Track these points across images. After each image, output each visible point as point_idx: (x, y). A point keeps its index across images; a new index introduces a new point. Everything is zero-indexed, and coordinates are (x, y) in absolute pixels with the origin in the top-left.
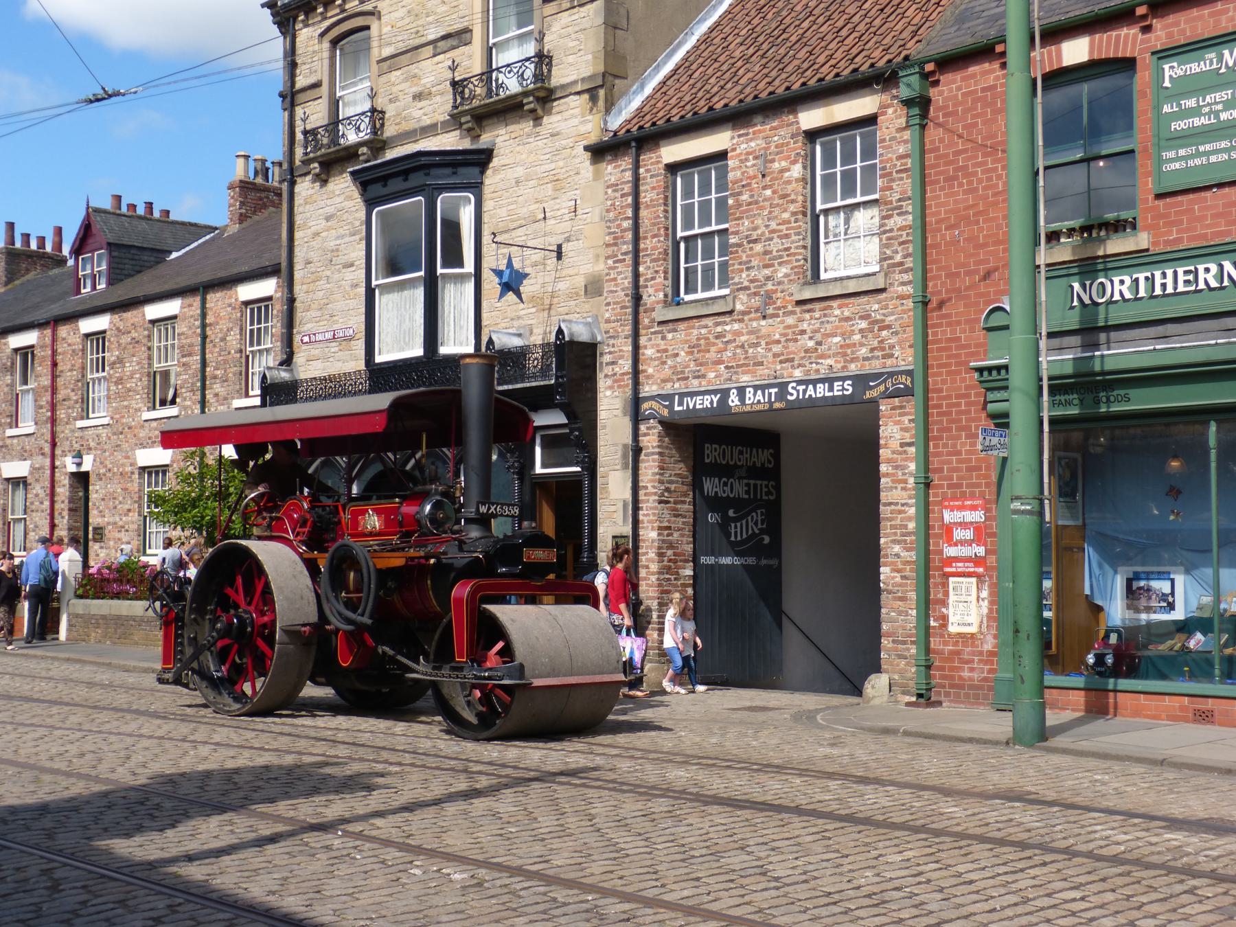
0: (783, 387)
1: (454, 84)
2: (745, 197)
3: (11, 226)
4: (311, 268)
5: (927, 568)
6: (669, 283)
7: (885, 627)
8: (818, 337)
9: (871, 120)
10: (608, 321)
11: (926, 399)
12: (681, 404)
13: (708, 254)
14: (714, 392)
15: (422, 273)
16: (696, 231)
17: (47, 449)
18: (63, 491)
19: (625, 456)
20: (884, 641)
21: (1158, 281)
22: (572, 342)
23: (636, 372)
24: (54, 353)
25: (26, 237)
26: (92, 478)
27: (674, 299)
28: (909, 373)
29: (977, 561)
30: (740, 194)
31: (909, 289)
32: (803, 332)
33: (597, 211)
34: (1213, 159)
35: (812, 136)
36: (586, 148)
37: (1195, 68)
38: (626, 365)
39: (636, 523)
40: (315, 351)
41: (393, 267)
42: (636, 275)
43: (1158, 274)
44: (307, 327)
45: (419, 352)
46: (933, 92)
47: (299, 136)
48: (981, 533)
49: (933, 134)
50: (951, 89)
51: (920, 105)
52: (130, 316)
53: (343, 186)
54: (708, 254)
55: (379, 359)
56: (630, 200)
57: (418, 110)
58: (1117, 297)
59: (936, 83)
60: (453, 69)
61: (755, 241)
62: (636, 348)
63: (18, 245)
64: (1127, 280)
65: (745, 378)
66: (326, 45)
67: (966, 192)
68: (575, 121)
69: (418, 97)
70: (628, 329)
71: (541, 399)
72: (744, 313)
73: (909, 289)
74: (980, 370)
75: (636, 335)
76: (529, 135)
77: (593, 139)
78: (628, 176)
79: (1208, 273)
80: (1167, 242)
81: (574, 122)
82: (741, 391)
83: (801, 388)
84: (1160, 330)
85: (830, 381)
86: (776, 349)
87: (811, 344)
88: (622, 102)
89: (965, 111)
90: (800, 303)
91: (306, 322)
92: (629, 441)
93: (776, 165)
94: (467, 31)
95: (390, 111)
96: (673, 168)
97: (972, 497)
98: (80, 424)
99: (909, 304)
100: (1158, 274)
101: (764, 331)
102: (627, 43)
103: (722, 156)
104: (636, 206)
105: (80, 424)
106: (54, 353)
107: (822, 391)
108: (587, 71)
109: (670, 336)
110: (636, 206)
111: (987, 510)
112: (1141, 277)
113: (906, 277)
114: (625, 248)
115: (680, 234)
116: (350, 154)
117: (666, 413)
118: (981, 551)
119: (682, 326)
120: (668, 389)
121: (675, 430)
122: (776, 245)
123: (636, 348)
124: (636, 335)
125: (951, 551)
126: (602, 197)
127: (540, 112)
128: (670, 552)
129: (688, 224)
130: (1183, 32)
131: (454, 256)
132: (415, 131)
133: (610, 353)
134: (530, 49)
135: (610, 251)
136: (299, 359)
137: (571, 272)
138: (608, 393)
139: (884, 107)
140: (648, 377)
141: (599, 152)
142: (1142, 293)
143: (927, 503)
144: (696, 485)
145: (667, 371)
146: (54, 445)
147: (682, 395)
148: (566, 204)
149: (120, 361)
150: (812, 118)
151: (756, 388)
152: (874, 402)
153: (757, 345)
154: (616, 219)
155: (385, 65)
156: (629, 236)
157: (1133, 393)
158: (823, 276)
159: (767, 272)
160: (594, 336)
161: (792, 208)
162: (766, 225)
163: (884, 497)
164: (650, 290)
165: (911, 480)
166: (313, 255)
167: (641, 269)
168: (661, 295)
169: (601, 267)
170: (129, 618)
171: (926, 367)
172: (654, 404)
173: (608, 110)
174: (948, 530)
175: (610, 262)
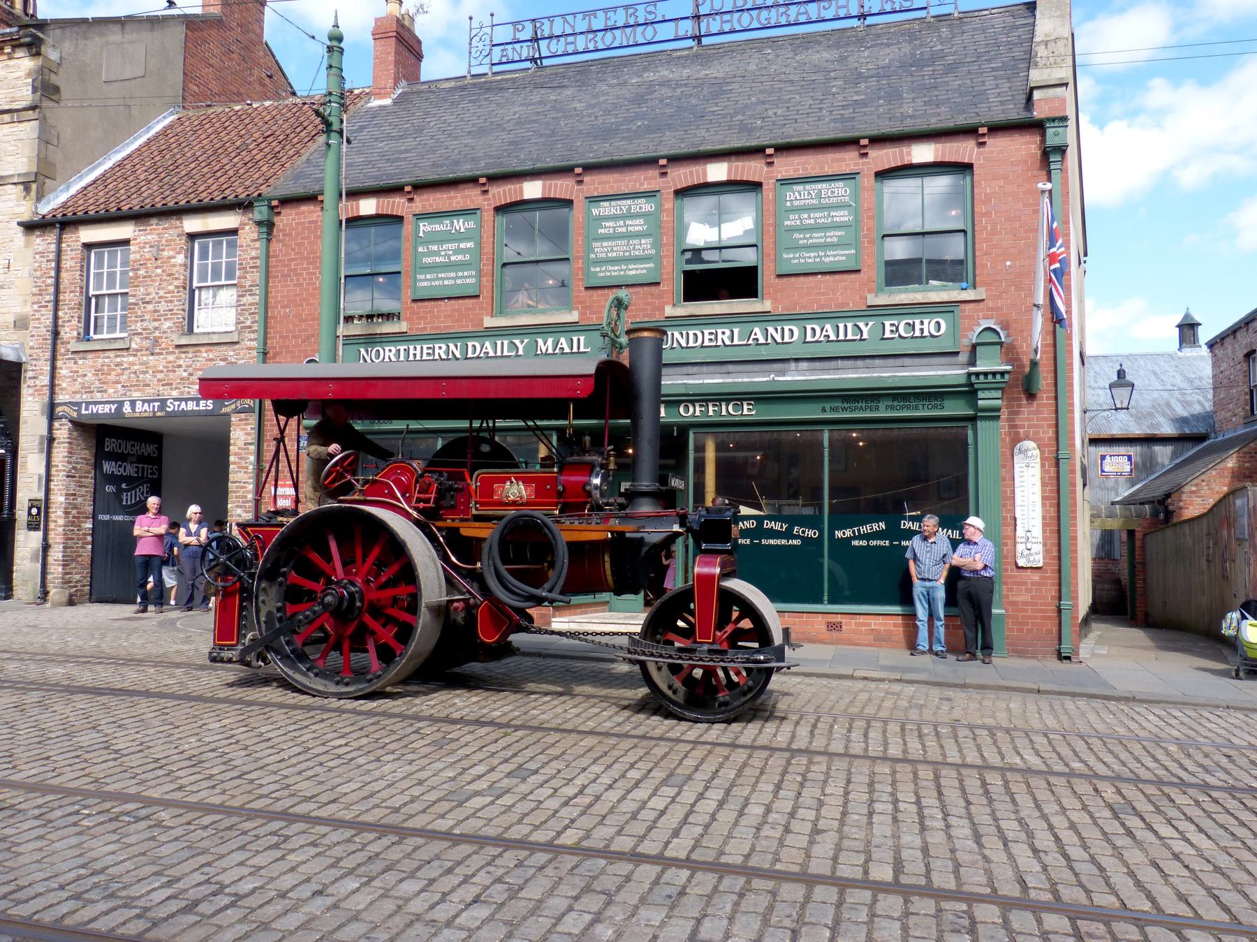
0: (163, 402)
2: (142, 272)
6: (82, 325)
8: (190, 370)
9: (234, 232)
10: (31, 348)
12: (87, 409)
14: (113, 402)
16: (104, 291)
19: (41, 443)
21: (412, 352)
23: (52, 386)
27: (85, 336)
30: (138, 269)
31: (254, 344)
32: (180, 366)
33: (27, 269)
34: (446, 282)
35: (192, 237)
36: (19, 224)
37: (437, 227)
38: (45, 380)
39: (48, 491)
42: (56, 318)
43: (412, 347)
49: (276, 246)
50: (288, 218)
51: (268, 226)
56: (53, 264)
58: (387, 359)
59: (279, 213)
61: (148, 303)
65: (136, 395)
67: (295, 285)
68: (11, 204)
70: (48, 355)
72: (137, 350)
73: (254, 344)
75: (54, 359)
78: (53, 247)
79: (440, 349)
80: (418, 329)
82: (133, 403)
83: (177, 403)
86: (160, 376)
87: (185, 374)
88: (51, 196)
89: (297, 234)
90: (178, 346)
93: (166, 253)
96: (88, 246)
99: (254, 353)
100: (412, 347)
101: (151, 364)
102: (56, 155)
103: (126, 242)
104: (58, 270)
108: (23, 170)
109: (80, 362)
110: (58, 270)
112: (402, 348)
113: (253, 336)
114: (48, 298)
115: (91, 293)
117: (75, 415)
119: (90, 356)
120: (77, 398)
121: (79, 426)
122: (163, 307)
124: (54, 359)
126: (31, 260)
128: (74, 512)
130: (431, 205)
135: (36, 299)
138: (30, 398)
139: (243, 224)
141: (29, 227)
142: (402, 358)
144: (97, 466)
145: (77, 386)
147: (88, 404)
150: (193, 224)
153: (146, 372)
154: (42, 276)
156: (52, 289)
158: (196, 330)
159: (156, 324)
160: (19, 357)
161: (176, 283)
163: (231, 476)
164: (67, 329)
167: (60, 314)
168: (75, 333)
169: (28, 309)
172: (66, 409)
175: (36, 307)
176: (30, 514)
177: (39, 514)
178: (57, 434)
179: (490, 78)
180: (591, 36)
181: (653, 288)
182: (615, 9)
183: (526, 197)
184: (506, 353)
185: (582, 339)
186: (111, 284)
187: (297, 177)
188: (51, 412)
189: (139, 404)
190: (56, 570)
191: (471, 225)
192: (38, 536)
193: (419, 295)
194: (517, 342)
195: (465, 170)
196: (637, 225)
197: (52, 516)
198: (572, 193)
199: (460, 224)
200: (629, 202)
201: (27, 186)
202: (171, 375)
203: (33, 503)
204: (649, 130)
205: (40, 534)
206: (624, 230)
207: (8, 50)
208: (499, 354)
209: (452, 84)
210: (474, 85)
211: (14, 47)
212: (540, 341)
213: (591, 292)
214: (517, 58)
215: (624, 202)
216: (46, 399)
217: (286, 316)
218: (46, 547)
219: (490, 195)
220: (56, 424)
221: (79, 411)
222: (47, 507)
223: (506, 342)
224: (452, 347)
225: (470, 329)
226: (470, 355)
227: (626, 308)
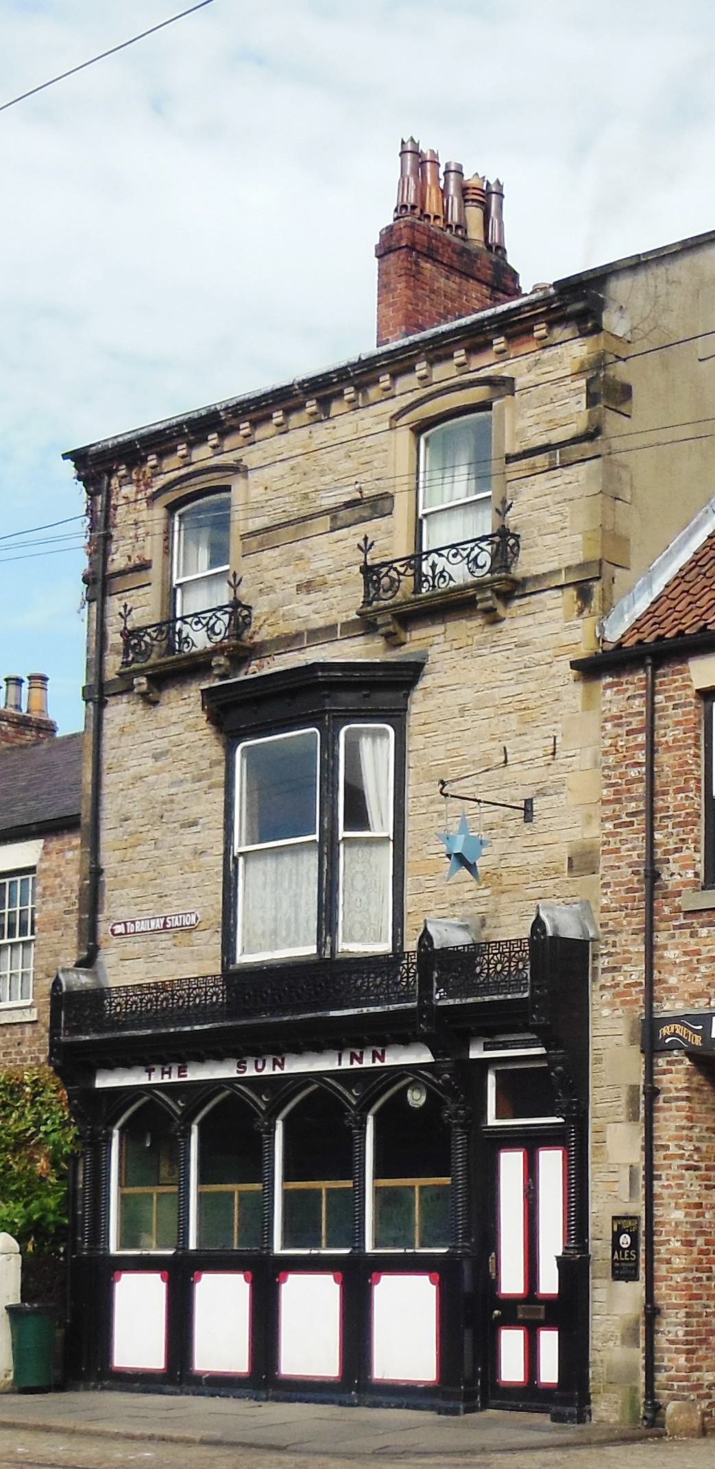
1: (367, 570)
4: (131, 826)
10: (605, 909)
15: (316, 837)
19: (633, 1102)
22: (556, 938)
23: (650, 983)
33: (589, 752)
36: (574, 665)
38: (636, 972)
39: (650, 1198)
40: (133, 946)
41: (265, 828)
42: (651, 845)
44: (122, 913)
45: (312, 950)
47: (114, 639)
53: (185, 707)
55: (244, 958)
56: (642, 738)
57: (307, 601)
60: (366, 547)
62: (650, 947)
66: (159, 512)
68: (555, 627)
69: (306, 587)
70: (638, 921)
71: (497, 1022)
75: (650, 930)
76: (481, 644)
77: (583, 652)
78: (639, 704)
81: (551, 629)
88: (625, 603)
91: (117, 905)
92: (640, 1080)
94: (387, 497)
95: (261, 607)
102: (628, 521)
104: (651, 748)
108: (577, 558)
110: (651, 748)
114: (632, 806)
116: (197, 666)
117: (698, 1041)
123: (650, 947)
124: (650, 930)
126: (595, 732)
127: (501, 611)
131: (358, 815)
132: (298, 636)
133: (609, 954)
134: (485, 523)
135: (609, 810)
136: (108, 957)
137: (546, 838)
138: (606, 1012)
140: (670, 990)
141: (591, 669)
148: (537, 745)
155: (254, 542)
156: (640, 789)
160: (585, 932)
164: (673, 867)
166: (135, 810)
167: (657, 836)
168: (690, 874)
169: (595, 832)
172: (679, 1029)
173: (605, 613)
175: (609, 826)
176: (616, 1246)
177: (634, 1245)
178: (664, 1081)
188: (651, 1037)
190: (673, 1361)
192: (630, 1295)
197: (662, 1252)
201: (584, 595)
203: (622, 1224)
205: (639, 1287)
207: (540, 330)
211: (551, 325)
216: (640, 1011)
218: (652, 1313)
220: (661, 1062)
221: (705, 1034)
222: (650, 1233)
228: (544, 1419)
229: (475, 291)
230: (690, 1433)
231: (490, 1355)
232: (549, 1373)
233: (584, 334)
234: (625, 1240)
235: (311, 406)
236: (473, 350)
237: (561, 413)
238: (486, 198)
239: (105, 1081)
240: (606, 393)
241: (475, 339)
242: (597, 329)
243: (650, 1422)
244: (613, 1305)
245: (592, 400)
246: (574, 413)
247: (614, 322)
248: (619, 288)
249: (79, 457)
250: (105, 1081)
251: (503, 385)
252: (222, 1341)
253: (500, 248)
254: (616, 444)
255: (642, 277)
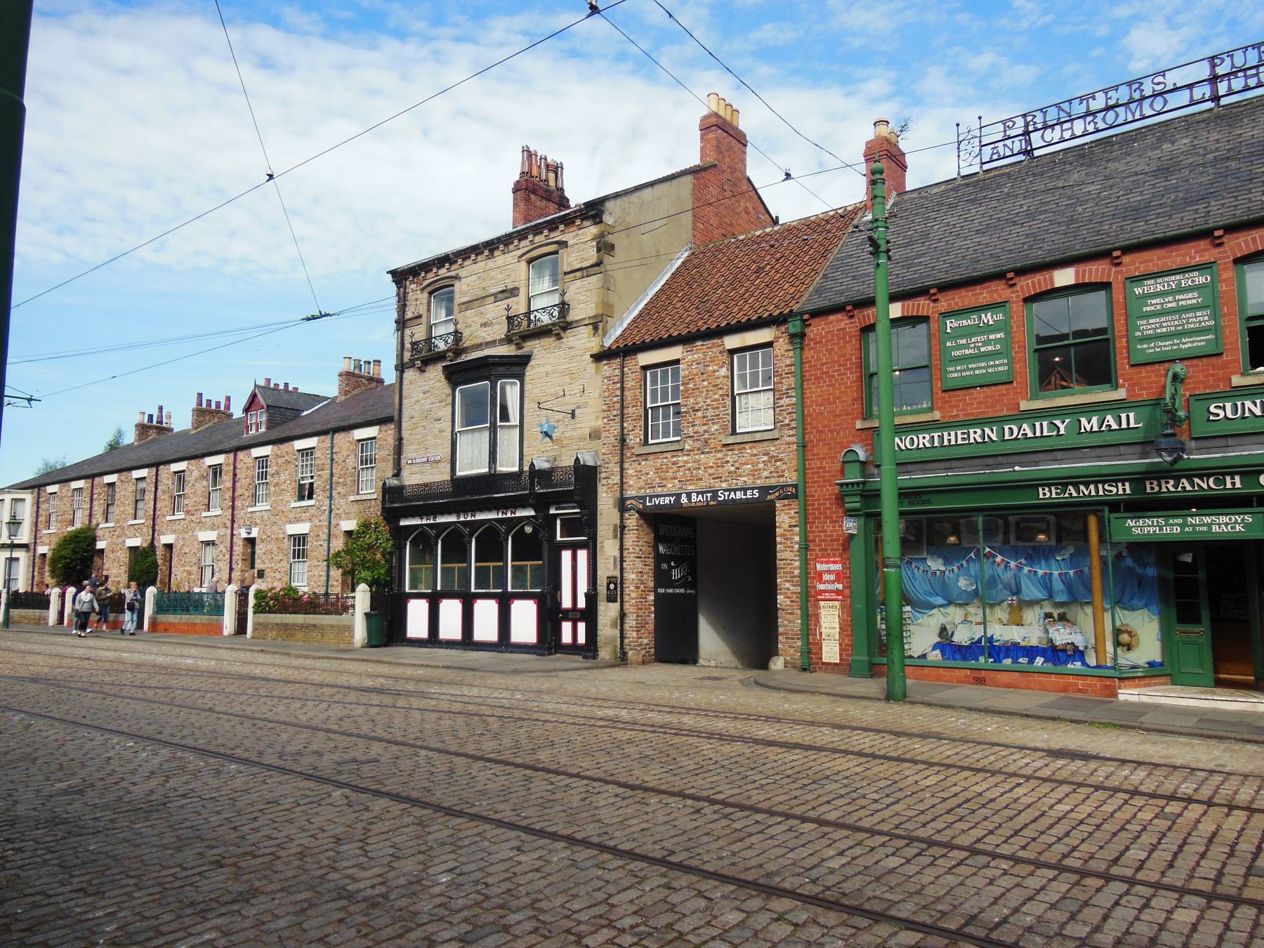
0: (715, 493)
1: (509, 318)
3: (200, 395)
4: (414, 421)
5: (807, 596)
7: (780, 630)
8: (737, 465)
9: (769, 345)
11: (806, 501)
13: (666, 417)
14: (672, 495)
17: (229, 524)
18: (239, 548)
19: (615, 531)
20: (780, 638)
23: (622, 483)
24: (235, 468)
25: (209, 402)
26: (257, 541)
28: (795, 486)
29: (838, 592)
31: (794, 439)
34: (977, 372)
35: (732, 352)
37: (965, 323)
38: (617, 479)
39: (622, 569)
40: (415, 469)
41: (468, 421)
42: (622, 428)
43: (946, 434)
44: (411, 455)
46: (807, 330)
47: (408, 346)
48: (839, 577)
49: (808, 354)
50: (818, 329)
51: (798, 338)
52: (285, 447)
53: (435, 373)
54: (666, 417)
55: (459, 473)
57: (484, 331)
60: (508, 309)
63: (204, 405)
64: (927, 437)
65: (691, 488)
66: (425, 295)
69: (484, 325)
70: (617, 458)
71: (561, 499)
73: (794, 439)
74: (842, 485)
75: (622, 462)
77: (595, 351)
78: (617, 372)
79: (975, 435)
81: (583, 341)
82: (689, 495)
84: (947, 464)
85: (745, 490)
86: (710, 471)
87: (733, 469)
89: (827, 341)
90: (725, 445)
91: (409, 452)
94: (517, 289)
95: (466, 333)
96: (645, 368)
97: (834, 556)
98: (250, 509)
99: (795, 447)
100: (946, 434)
102: (613, 298)
103: (677, 362)
105: (250, 509)
106: (235, 468)
107: (739, 495)
111: (844, 564)
112: (936, 435)
113: (791, 432)
116: (441, 357)
118: (840, 586)
119: (651, 457)
120: (642, 493)
121: (645, 515)
122: (710, 413)
124: (622, 462)
125: (821, 587)
126: (600, 383)
129: (654, 400)
131: (505, 416)
132: (481, 344)
134: (556, 299)
136: (405, 473)
139: (777, 338)
141: (598, 358)
142: (936, 444)
143: (807, 560)
144: (656, 549)
145: (642, 483)
146: (233, 521)
147: (651, 497)
148: (577, 388)
149: (277, 473)
150: (732, 342)
151: (698, 493)
152: (772, 503)
155: (463, 307)
156: (618, 406)
157: (933, 497)
159: (705, 428)
161: (720, 392)
162: (703, 400)
165: (797, 547)
166: (416, 415)
169: (600, 423)
170: (294, 625)
171: (805, 482)
173: (604, 335)
174: (820, 575)
176: (608, 588)
177: (616, 588)
178: (628, 522)
179: (981, 176)
180: (1089, 119)
181: (1214, 359)
182: (1116, 88)
183: (1057, 285)
184: (1045, 433)
185: (1132, 415)
186: (665, 398)
187: (818, 291)
189: (694, 496)
190: (631, 635)
191: (1000, 317)
193: (950, 385)
194: (1058, 422)
195: (988, 267)
196: (1190, 299)
197: (627, 591)
198: (1109, 276)
199: (988, 318)
200: (1178, 277)
201: (596, 328)
202: (721, 470)
203: (611, 580)
204: (1187, 202)
205: (617, 605)
206: (1174, 305)
207: (578, 222)
208: (1038, 434)
209: (943, 188)
210: (967, 185)
212: (1084, 421)
213: (1138, 369)
214: (1008, 153)
215: (1173, 278)
216: (618, 495)
217: (821, 414)
218: (623, 615)
219: (1018, 287)
220: (626, 515)
221: (644, 504)
222: (622, 583)
223: (1045, 424)
224: (987, 430)
225: (1005, 413)
226: (1007, 437)
227: (1182, 381)
228: (580, 658)
229: (552, 206)
230: (638, 663)
231: (558, 632)
232: (582, 639)
233: (596, 224)
234: (612, 586)
235: (486, 252)
236: (551, 230)
237: (586, 255)
238: (556, 169)
239: (404, 523)
240: (605, 247)
241: (552, 226)
242: (601, 222)
243: (622, 659)
244: (607, 612)
245: (599, 250)
246: (591, 255)
247: (608, 219)
248: (610, 205)
249: (393, 273)
250: (404, 523)
251: (563, 244)
252: (451, 626)
253: (562, 189)
254: (609, 267)
255: (619, 201)
